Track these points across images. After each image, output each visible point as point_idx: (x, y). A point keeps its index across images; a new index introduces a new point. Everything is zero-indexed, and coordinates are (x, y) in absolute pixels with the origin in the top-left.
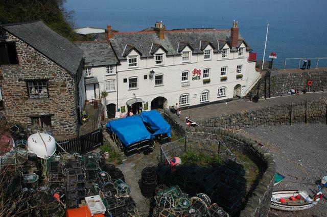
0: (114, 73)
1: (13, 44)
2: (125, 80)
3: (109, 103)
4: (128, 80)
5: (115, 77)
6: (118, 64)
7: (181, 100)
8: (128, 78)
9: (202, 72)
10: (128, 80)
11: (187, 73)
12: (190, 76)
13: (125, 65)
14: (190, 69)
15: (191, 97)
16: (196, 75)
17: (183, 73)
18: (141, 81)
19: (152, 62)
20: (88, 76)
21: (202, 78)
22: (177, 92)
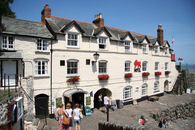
0: (48, 50)
2: (62, 63)
3: (36, 93)
4: (66, 64)
5: (48, 57)
6: (54, 40)
7: (125, 94)
10: (66, 64)
11: (129, 64)
12: (132, 67)
13: (62, 44)
14: (132, 59)
15: (133, 90)
16: (137, 68)
17: (126, 64)
19: (94, 46)
20: (8, 48)
22: (121, 84)
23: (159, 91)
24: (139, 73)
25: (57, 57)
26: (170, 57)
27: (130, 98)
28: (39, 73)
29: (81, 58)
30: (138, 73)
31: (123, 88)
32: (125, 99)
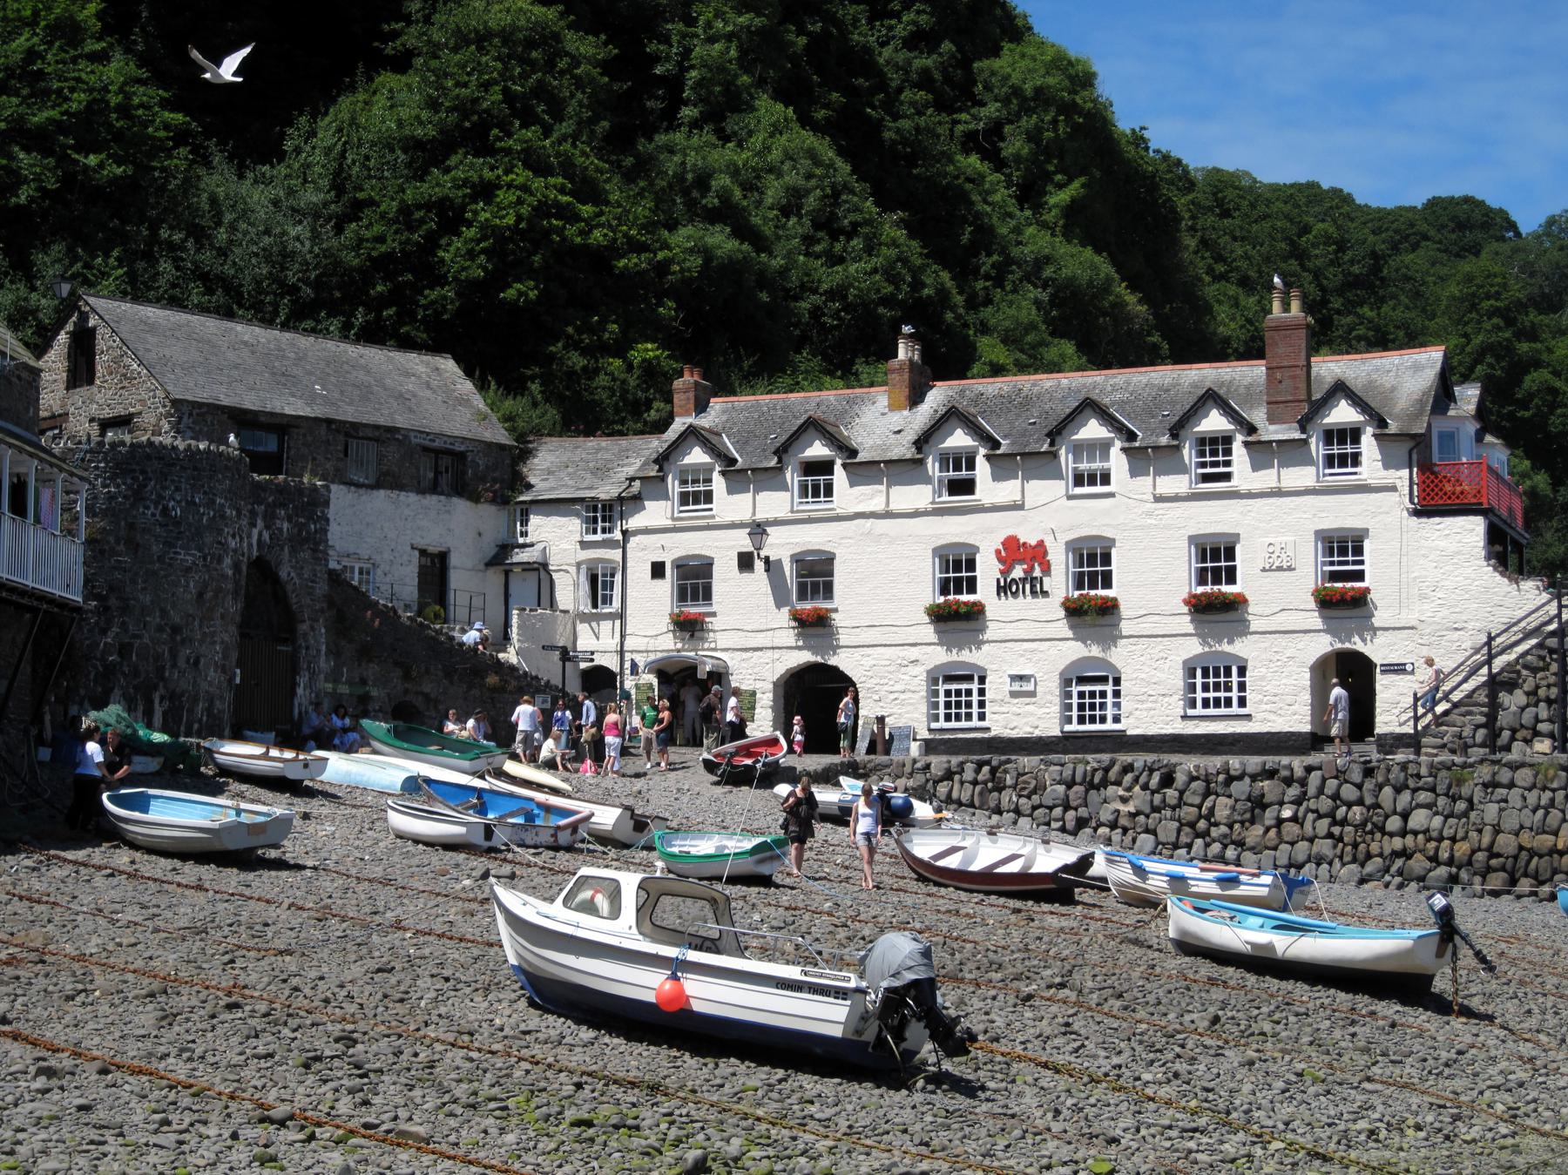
1: (94, 329)
2: (658, 570)
8: (668, 558)
9: (1059, 558)
12: (987, 571)
15: (997, 686)
18: (725, 577)
21: (1059, 584)
22: (913, 653)
23: (1248, 717)
24: (1041, 601)
25: (642, 553)
26: (754, 513)
27: (975, 723)
28: (595, 606)
29: (723, 549)
30: (1024, 605)
31: (920, 672)
32: (942, 724)
